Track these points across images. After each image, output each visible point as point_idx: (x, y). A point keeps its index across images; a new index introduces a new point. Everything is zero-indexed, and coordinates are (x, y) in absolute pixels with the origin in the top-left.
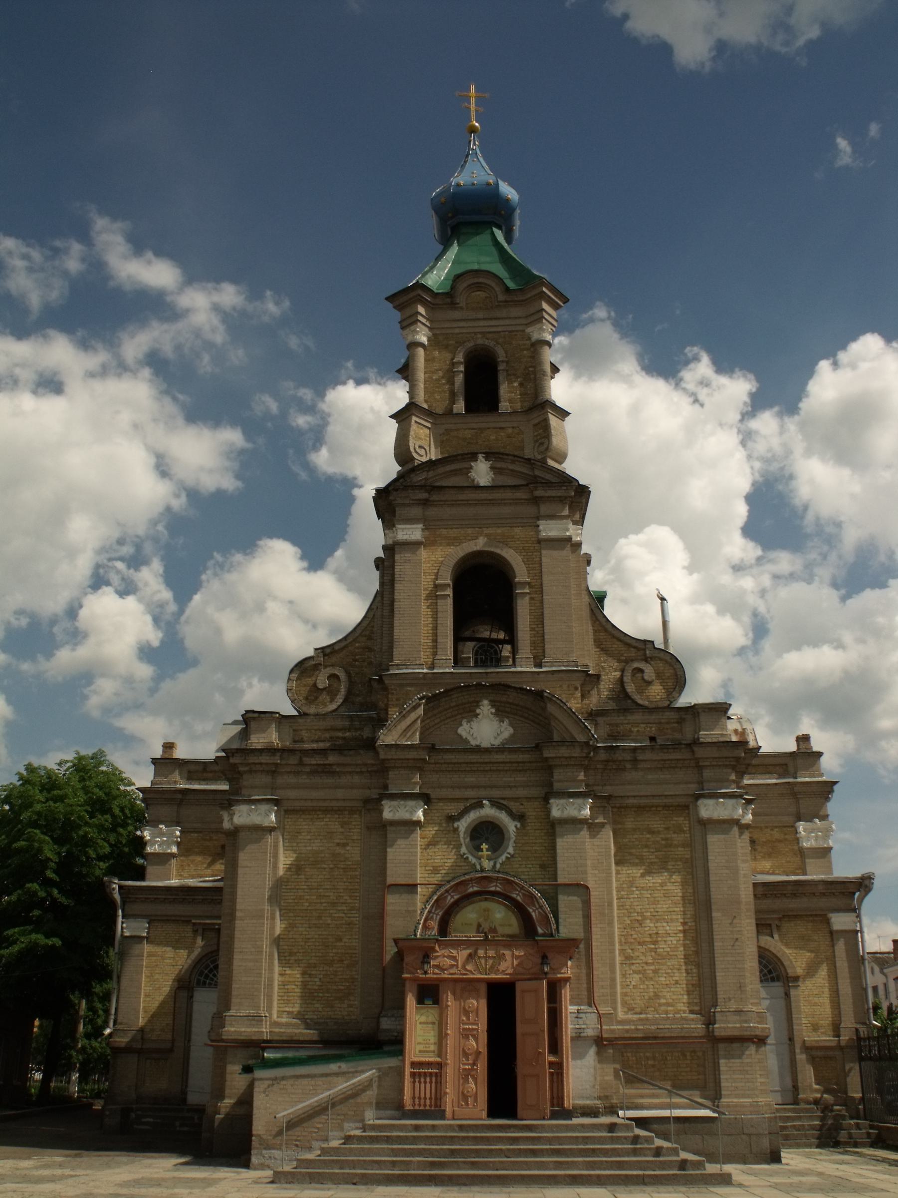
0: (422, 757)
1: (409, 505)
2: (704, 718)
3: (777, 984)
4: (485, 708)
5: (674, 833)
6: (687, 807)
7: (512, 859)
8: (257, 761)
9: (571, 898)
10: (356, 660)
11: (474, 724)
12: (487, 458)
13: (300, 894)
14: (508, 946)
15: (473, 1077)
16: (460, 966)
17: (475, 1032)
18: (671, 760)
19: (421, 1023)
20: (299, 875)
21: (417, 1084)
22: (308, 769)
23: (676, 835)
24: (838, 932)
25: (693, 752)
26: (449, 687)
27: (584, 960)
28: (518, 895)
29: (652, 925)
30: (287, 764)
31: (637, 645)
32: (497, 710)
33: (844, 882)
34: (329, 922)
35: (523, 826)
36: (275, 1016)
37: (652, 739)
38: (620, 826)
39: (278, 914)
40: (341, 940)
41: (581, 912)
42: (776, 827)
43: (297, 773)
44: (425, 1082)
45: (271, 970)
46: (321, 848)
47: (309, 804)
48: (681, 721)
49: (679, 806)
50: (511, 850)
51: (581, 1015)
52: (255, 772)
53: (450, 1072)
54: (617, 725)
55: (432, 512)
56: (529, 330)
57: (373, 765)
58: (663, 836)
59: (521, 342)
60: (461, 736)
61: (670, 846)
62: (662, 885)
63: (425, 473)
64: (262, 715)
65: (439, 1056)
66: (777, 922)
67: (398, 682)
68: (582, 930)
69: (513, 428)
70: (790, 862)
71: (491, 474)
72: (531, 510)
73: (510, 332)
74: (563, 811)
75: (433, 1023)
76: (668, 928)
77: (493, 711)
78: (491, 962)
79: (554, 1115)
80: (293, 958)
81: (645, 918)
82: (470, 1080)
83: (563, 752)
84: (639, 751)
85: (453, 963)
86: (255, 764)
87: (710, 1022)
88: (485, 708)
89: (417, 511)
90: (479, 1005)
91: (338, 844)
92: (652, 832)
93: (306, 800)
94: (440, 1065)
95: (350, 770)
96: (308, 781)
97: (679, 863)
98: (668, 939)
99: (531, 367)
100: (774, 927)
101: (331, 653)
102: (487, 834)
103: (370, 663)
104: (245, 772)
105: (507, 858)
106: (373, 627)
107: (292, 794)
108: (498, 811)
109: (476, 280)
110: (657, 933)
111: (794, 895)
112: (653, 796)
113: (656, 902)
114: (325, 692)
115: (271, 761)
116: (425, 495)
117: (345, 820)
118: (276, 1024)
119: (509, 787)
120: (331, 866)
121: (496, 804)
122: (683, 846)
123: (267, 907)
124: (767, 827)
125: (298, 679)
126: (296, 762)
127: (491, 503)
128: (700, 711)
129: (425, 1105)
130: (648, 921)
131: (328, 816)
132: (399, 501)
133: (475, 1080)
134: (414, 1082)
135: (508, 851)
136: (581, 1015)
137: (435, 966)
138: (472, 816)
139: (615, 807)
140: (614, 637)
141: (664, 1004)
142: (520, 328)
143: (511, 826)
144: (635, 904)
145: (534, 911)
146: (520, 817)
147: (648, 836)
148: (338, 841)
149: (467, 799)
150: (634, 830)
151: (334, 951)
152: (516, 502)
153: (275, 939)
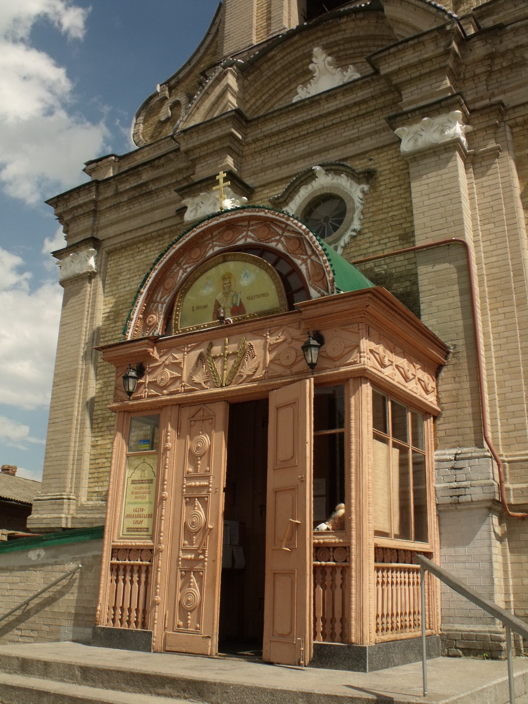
0: (227, 131)
7: (359, 238)
9: (437, 267)
14: (258, 332)
15: (196, 573)
16: (185, 378)
17: (204, 493)
19: (133, 482)
20: (116, 322)
21: (121, 583)
22: (125, 198)
27: (465, 366)
28: (278, 241)
35: (373, 188)
36: (83, 499)
39: (92, 372)
41: (456, 287)
43: (116, 206)
44: (132, 582)
45: (81, 441)
50: (356, 225)
51: (460, 464)
53: (164, 568)
64: (99, 163)
65: (152, 538)
68: (460, 316)
74: (416, 140)
75: (150, 481)
78: (231, 362)
79: (322, 658)
80: (106, 424)
82: (193, 580)
85: (177, 374)
90: (215, 444)
94: (150, 552)
95: (166, 183)
96: (128, 211)
107: (111, 231)
108: (337, 177)
114: (168, 124)
115: (88, 199)
118: (81, 508)
121: (332, 168)
123: (81, 365)
125: (145, 121)
129: (129, 622)
131: (149, 246)
133: (200, 579)
134: (117, 581)
135: (352, 227)
136: (460, 464)
137: (153, 384)
138: (304, 194)
139: (517, 125)
145: (304, 261)
146: (368, 176)
153: (87, 403)
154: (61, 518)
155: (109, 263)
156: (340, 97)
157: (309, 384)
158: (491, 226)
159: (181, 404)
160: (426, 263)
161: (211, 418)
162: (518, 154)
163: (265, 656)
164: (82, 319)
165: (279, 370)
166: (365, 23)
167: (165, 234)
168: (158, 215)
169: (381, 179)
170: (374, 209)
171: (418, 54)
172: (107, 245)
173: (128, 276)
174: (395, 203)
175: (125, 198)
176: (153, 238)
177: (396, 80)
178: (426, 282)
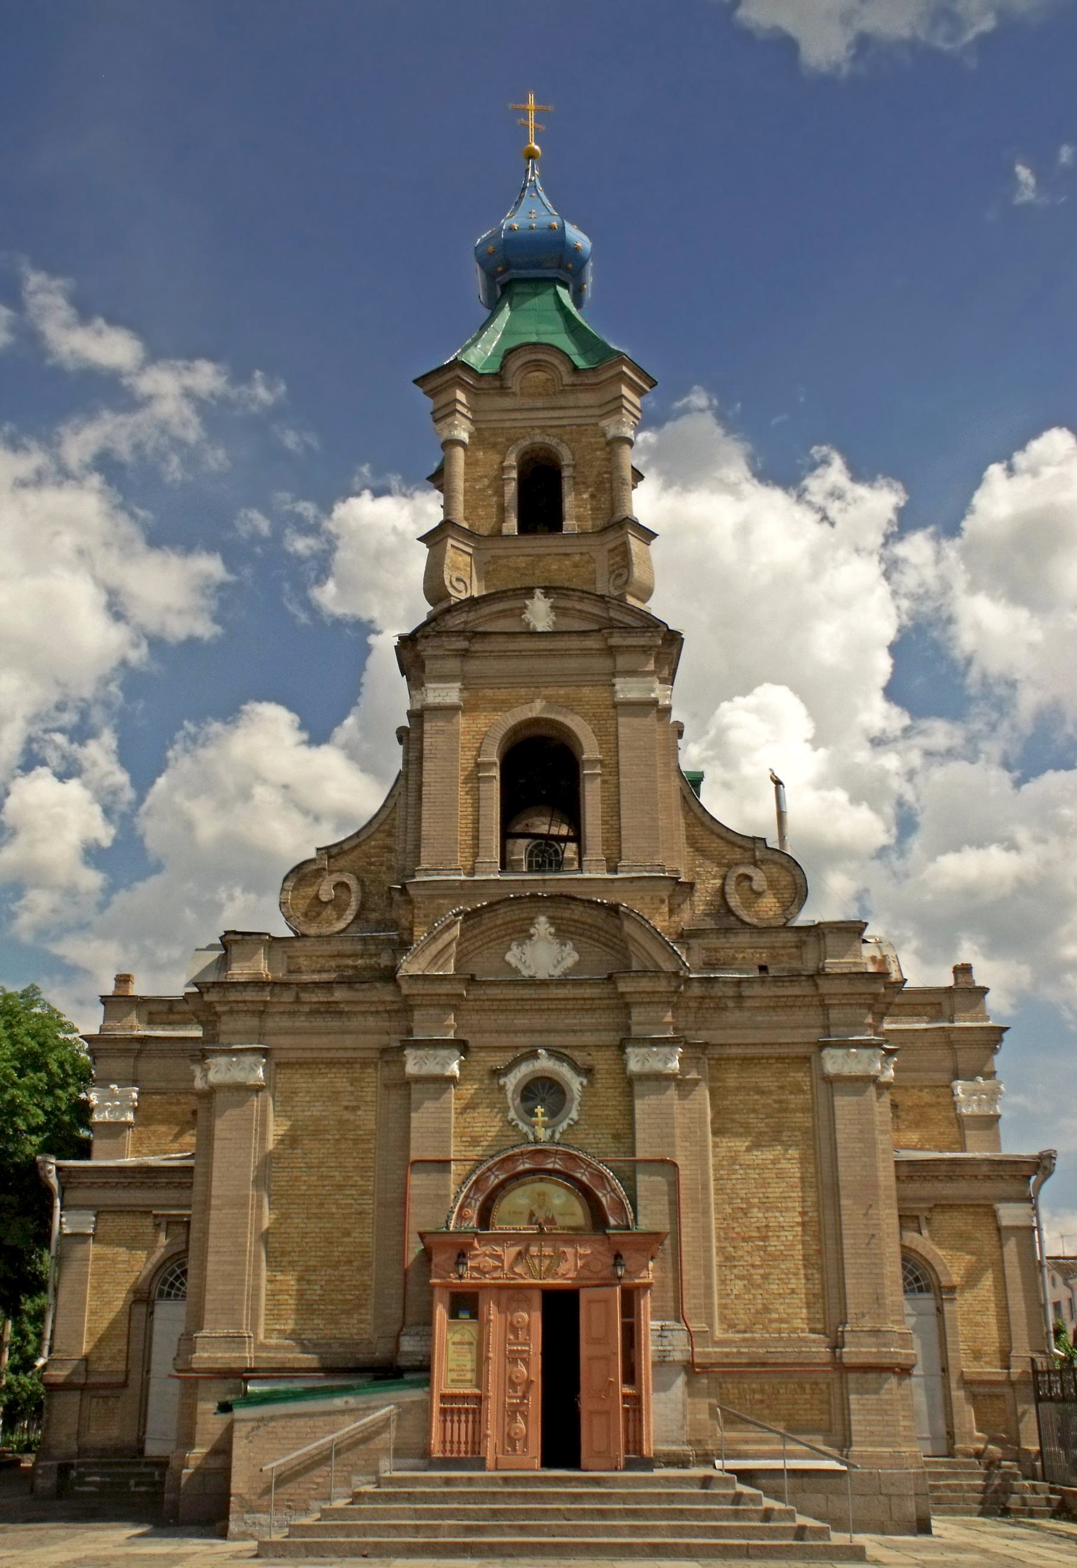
0: (458, 992)
1: (443, 657)
2: (831, 941)
3: (926, 1295)
4: (542, 926)
5: (791, 1093)
6: (807, 1059)
8: (239, 999)
9: (653, 1178)
10: (371, 864)
11: (527, 948)
12: (546, 595)
13: (296, 1174)
14: (570, 1242)
15: (522, 1413)
16: (506, 1267)
17: (525, 1355)
18: (788, 996)
19: (454, 1343)
20: (294, 1149)
21: (449, 1424)
22: (306, 1008)
23: (793, 1096)
24: (1007, 1228)
25: (816, 985)
26: (494, 899)
27: (670, 1260)
28: (583, 1174)
29: (760, 1215)
30: (279, 1002)
31: (743, 843)
32: (558, 930)
33: (1016, 1162)
34: (334, 1210)
36: (261, 1337)
37: (763, 968)
38: (719, 1084)
39: (266, 1200)
40: (349, 1234)
41: (666, 1198)
42: (926, 1087)
43: (292, 1014)
44: (459, 1421)
45: (257, 1275)
46: (324, 1114)
47: (307, 1054)
48: (800, 945)
49: (797, 1057)
50: (574, 1115)
51: (666, 1333)
52: (238, 1012)
53: (492, 1408)
54: (716, 950)
55: (473, 666)
56: (603, 423)
57: (393, 1002)
58: (775, 1097)
59: (593, 440)
60: (509, 964)
61: (786, 1110)
62: (774, 1162)
63: (464, 615)
64: (247, 938)
65: (478, 1386)
66: (926, 1214)
67: (427, 892)
68: (667, 1222)
69: (581, 554)
70: (944, 1133)
71: (552, 616)
72: (602, 664)
73: (579, 426)
74: (643, 1064)
75: (471, 1344)
76: (782, 1219)
77: (552, 930)
78: (547, 1262)
79: (629, 1465)
80: (286, 1259)
81: (751, 1206)
82: (519, 1418)
83: (645, 985)
84: (745, 984)
85: (497, 1263)
86: (237, 1002)
87: (836, 1345)
88: (542, 926)
89: (452, 665)
90: (532, 1319)
91: (346, 1108)
92: (761, 1092)
93: (304, 1049)
94: (479, 1399)
95: (363, 1009)
96: (306, 1024)
97: (797, 1133)
98: (782, 1233)
99: (606, 472)
100: (922, 1220)
101: (339, 854)
102: (543, 1092)
103: (390, 868)
104: (224, 1013)
105: (569, 1125)
106: (394, 819)
108: (558, 1063)
109: (534, 357)
110: (767, 1226)
111: (950, 1178)
112: (764, 1044)
113: (765, 1185)
114: (330, 907)
115: (259, 999)
116: (464, 644)
117: (356, 1075)
118: (263, 1347)
119: (573, 1031)
120: (337, 1137)
121: (555, 1054)
122: (803, 1110)
123: (251, 1192)
124: (913, 1087)
125: (294, 889)
126: (291, 1000)
127: (551, 653)
128: (826, 931)
129: (459, 1452)
130: (755, 1210)
131: (334, 1070)
132: (430, 652)
133: (525, 1418)
134: (445, 1421)
135: (571, 1116)
136: (666, 1333)
137: (473, 1268)
138: (524, 1071)
139: (713, 1059)
140: (712, 832)
141: (776, 1320)
142: (593, 421)
143: (575, 1083)
144: (738, 1187)
145: (605, 1195)
146: (588, 1072)
147: (756, 1097)
148: (346, 1104)
149: (517, 1048)
150: (738, 1089)
151: (340, 1249)
152: (585, 653)
153: (263, 1234)
154: (246, 1358)
155: (278, 1076)
156: (569, 987)
157: (618, 1289)
158: (688, 1144)
159: (501, 1287)
160: (644, 1173)
161: (529, 1300)
162: (712, 1085)
163: (582, 1467)
164: (250, 1139)
165: (587, 1273)
166: (595, 913)
167: (356, 1063)
168: (349, 1041)
169: (598, 1076)
170: (591, 1103)
171: (652, 984)
172: (279, 1056)
173: (307, 1099)
174: (610, 1103)
175: (306, 1008)
176: (339, 1063)
177: (629, 999)
178: (643, 1188)
